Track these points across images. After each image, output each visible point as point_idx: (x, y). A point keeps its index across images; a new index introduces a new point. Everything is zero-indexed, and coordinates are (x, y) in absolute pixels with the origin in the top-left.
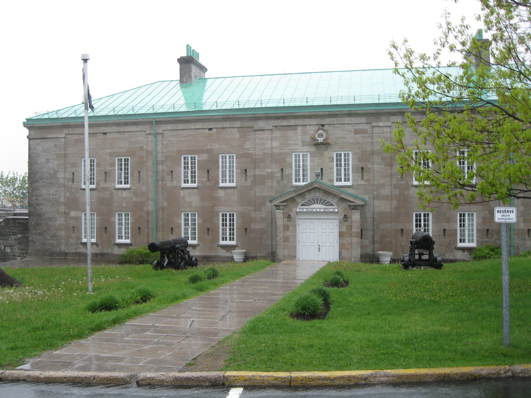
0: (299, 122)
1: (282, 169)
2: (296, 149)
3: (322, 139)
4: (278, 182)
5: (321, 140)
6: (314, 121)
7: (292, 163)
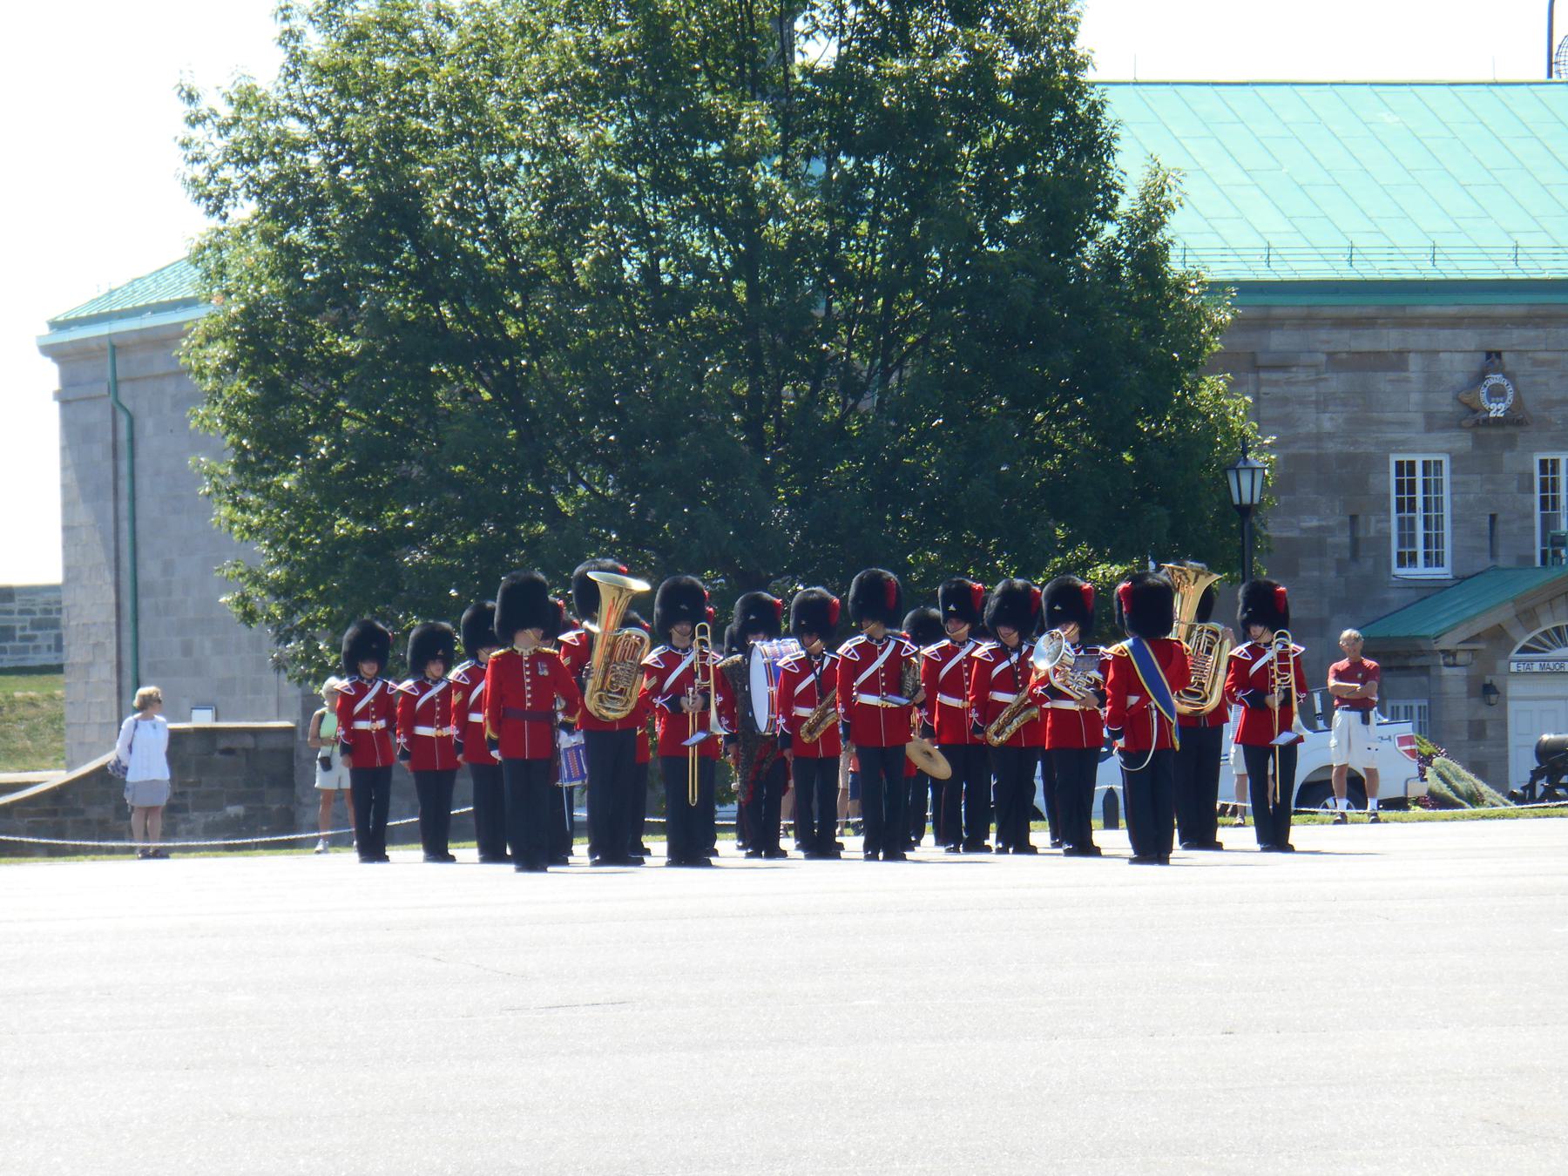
0: (1418, 338)
1: (1353, 518)
2: (1403, 442)
3: (1502, 406)
4: (1341, 566)
5: (1497, 409)
6: (1470, 339)
7: (1388, 496)
